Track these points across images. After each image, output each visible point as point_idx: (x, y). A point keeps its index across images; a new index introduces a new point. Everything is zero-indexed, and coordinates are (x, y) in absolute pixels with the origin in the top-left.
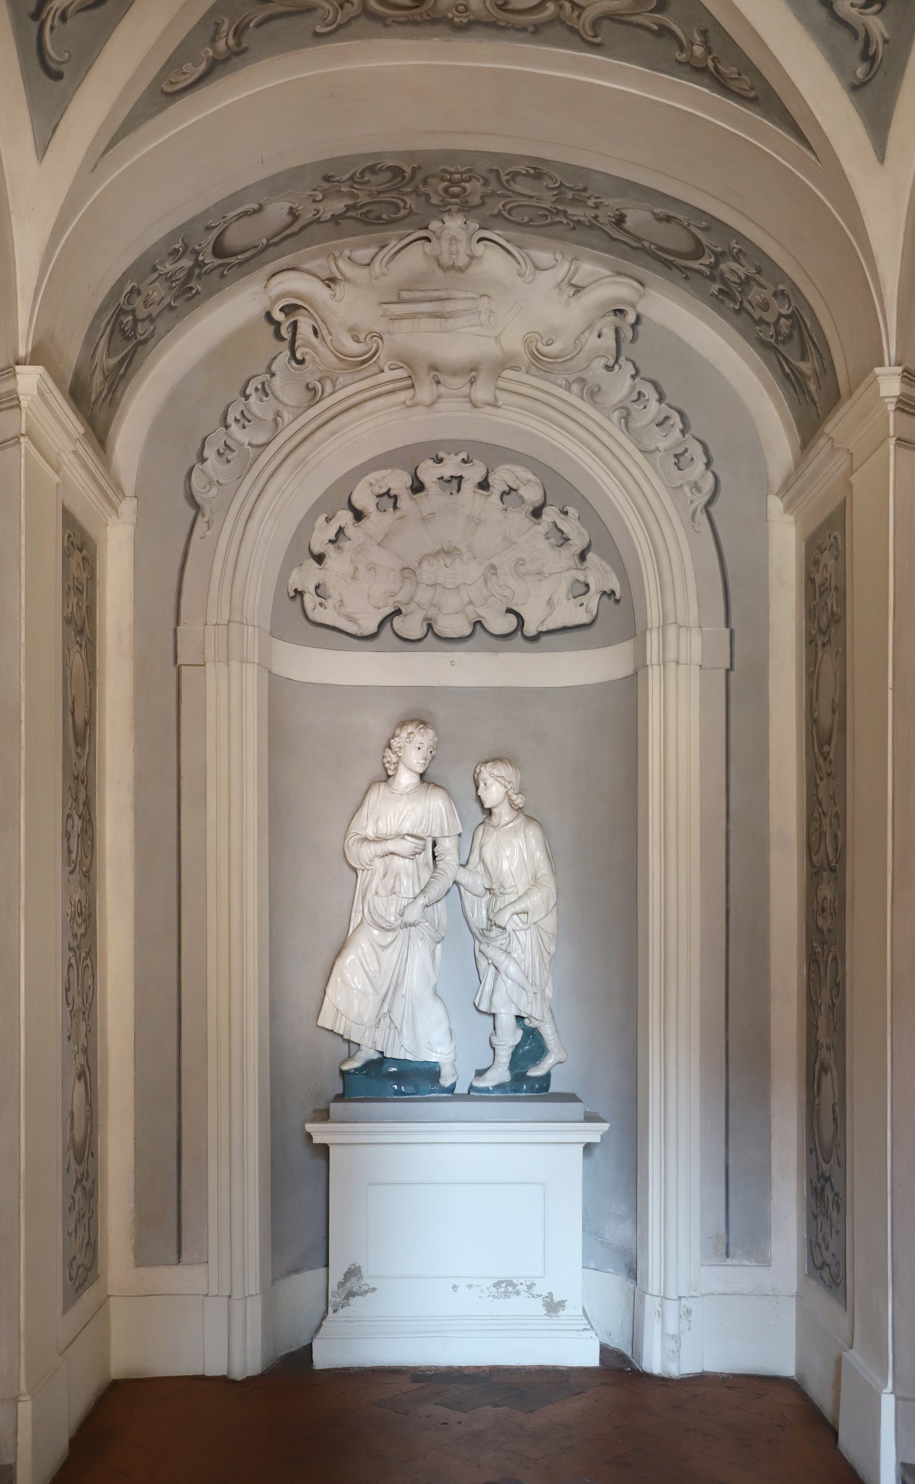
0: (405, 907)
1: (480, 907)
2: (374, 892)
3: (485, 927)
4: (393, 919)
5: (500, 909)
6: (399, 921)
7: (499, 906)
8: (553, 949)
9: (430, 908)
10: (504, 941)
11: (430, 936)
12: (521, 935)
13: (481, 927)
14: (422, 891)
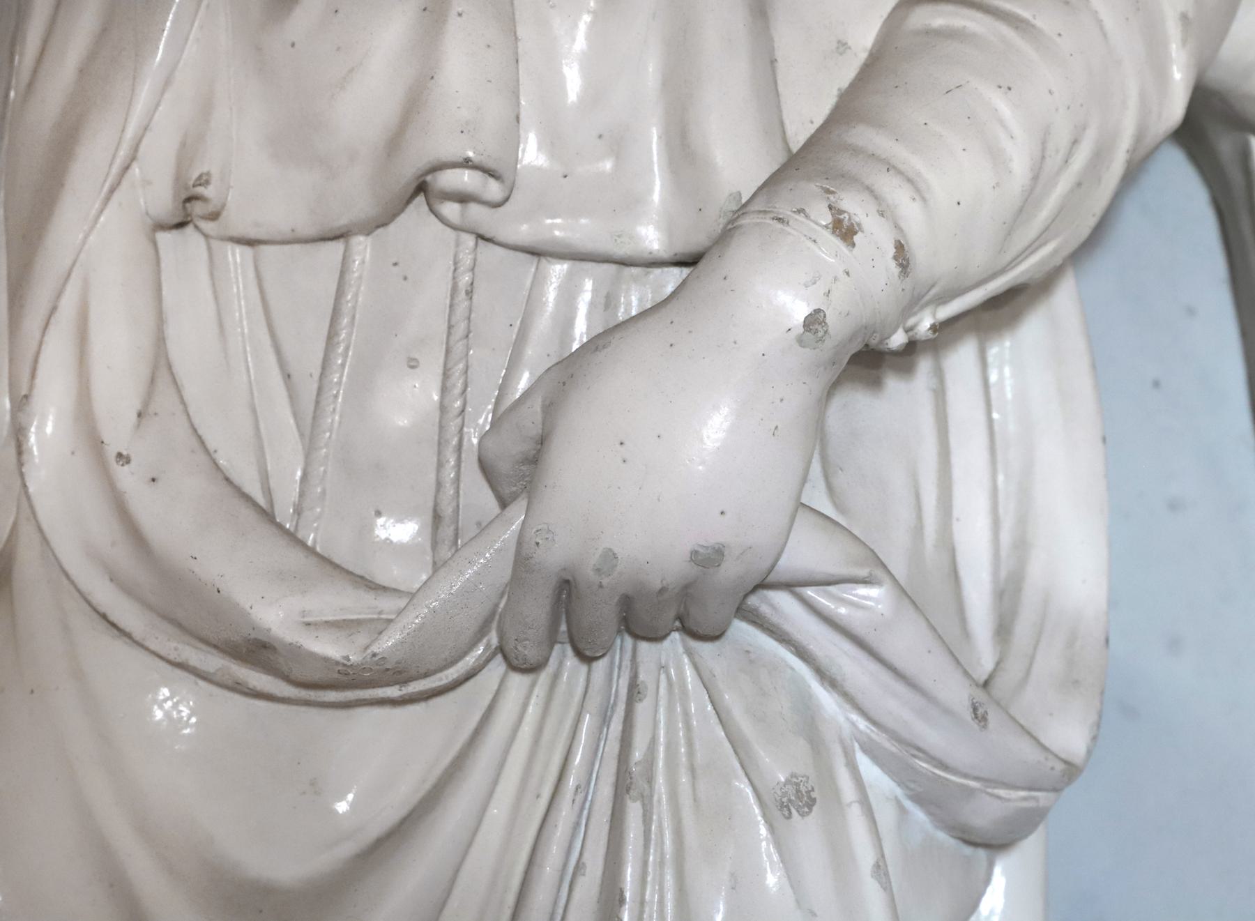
0: (570, 371)
2: (162, 200)
4: (400, 531)
6: (484, 563)
9: (905, 397)
11: (903, 757)
14: (810, 163)
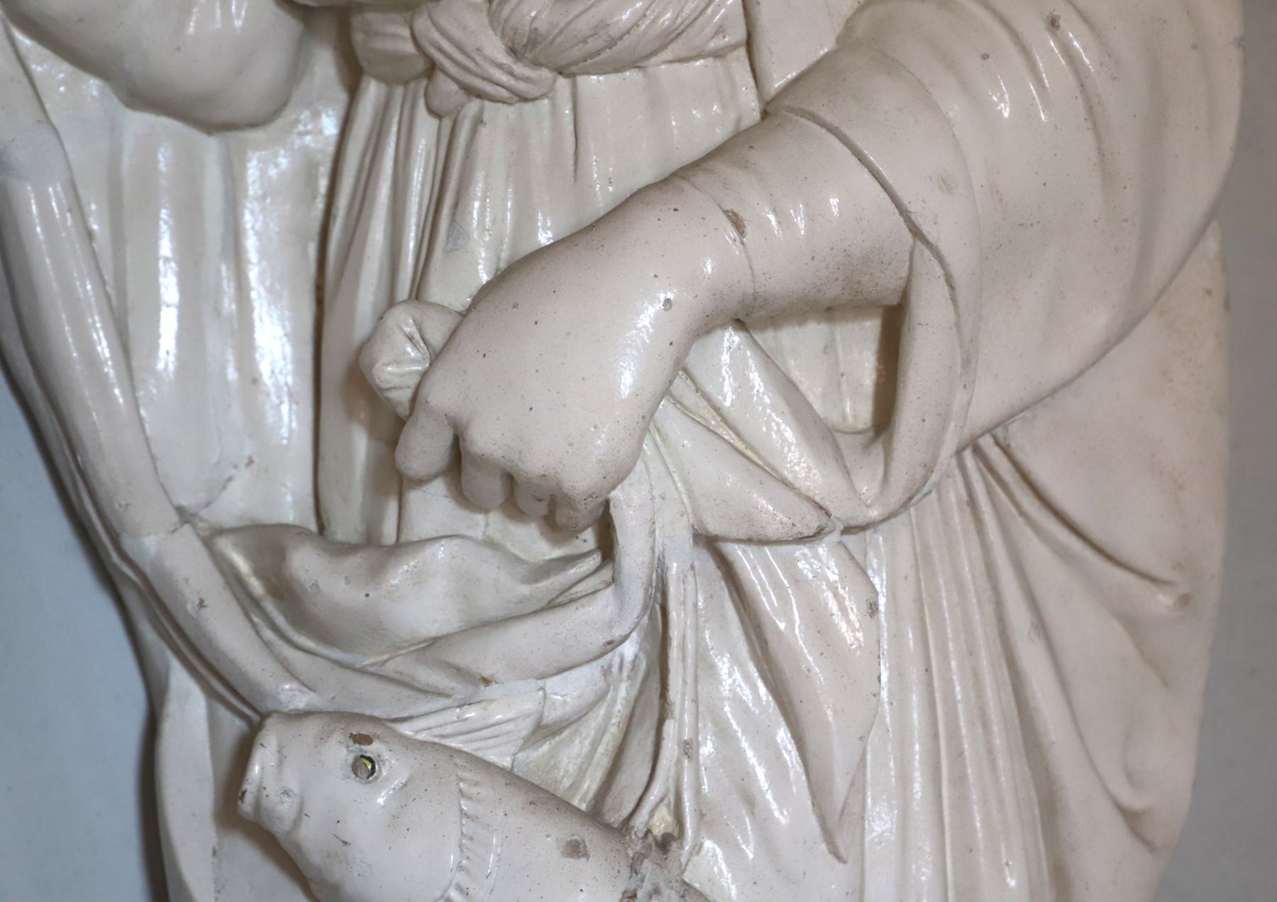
1: (214, 249)
3: (289, 502)
5: (514, 272)
7: (487, 232)
8: (1169, 768)
10: (567, 692)
12: (814, 593)
13: (235, 503)
